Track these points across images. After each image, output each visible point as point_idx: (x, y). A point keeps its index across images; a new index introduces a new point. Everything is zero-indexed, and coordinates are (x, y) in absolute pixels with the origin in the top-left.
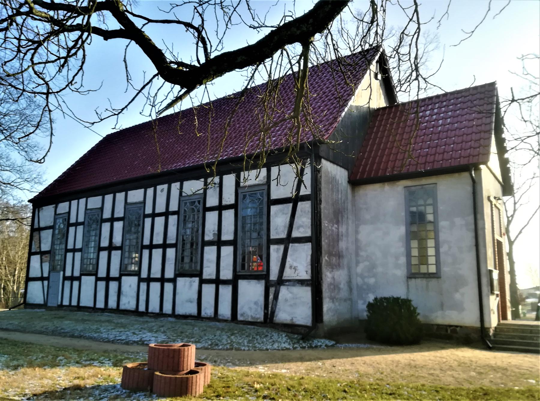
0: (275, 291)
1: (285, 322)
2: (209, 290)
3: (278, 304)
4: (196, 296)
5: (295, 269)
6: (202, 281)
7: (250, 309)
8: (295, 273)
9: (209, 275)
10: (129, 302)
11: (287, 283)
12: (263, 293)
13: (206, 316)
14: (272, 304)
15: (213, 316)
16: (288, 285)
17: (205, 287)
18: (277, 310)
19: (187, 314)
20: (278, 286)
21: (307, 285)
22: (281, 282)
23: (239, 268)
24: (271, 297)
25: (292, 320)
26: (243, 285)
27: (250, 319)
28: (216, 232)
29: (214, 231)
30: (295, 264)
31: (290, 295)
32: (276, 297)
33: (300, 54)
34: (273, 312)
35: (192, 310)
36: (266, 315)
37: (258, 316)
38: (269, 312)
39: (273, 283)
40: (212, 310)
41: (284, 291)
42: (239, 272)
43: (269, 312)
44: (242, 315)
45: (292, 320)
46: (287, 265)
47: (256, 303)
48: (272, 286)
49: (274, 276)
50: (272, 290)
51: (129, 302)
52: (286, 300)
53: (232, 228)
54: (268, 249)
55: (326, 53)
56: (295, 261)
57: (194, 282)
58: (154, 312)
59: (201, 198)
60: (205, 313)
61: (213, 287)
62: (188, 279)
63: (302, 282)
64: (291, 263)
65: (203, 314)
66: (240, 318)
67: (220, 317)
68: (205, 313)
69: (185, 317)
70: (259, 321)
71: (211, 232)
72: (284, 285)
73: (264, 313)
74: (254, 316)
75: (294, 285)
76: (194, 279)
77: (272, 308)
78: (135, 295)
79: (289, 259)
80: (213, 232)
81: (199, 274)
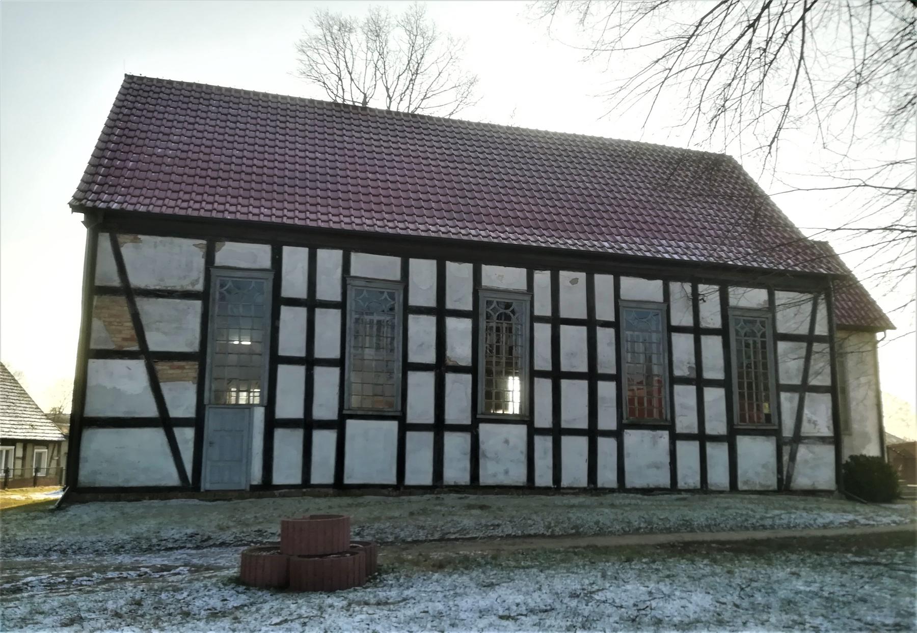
0: (791, 450)
1: (806, 488)
2: (688, 452)
3: (796, 466)
4: (667, 460)
5: (815, 423)
6: (675, 437)
7: (757, 474)
8: (815, 428)
9: (687, 427)
10: (507, 472)
11: (806, 441)
12: (775, 453)
13: (686, 487)
14: (788, 467)
15: (699, 486)
16: (807, 443)
17: (681, 445)
18: (795, 473)
19: (651, 486)
20: (794, 445)
21: (830, 443)
22: (798, 438)
23: (736, 419)
24: (786, 458)
25: (814, 484)
26: (744, 443)
27: (758, 488)
28: (694, 366)
29: (689, 363)
30: (814, 418)
31: (811, 455)
32: (793, 458)
33: (879, 345)
34: (789, 477)
35: (518, 476)
36: (780, 481)
37: (769, 483)
38: (785, 478)
39: (787, 440)
40: (698, 478)
41: (803, 452)
42: (738, 425)
43: (785, 478)
44: (746, 483)
45: (814, 484)
46: (805, 418)
47: (764, 466)
48: (786, 444)
49: (788, 431)
50: (786, 450)
51: (507, 472)
52: (806, 462)
53: (721, 362)
54: (778, 396)
55: (758, 18)
56: (814, 413)
57: (661, 437)
58: (575, 486)
59: (661, 310)
60: (685, 484)
61: (695, 446)
62: (647, 433)
63: (823, 440)
64: (809, 415)
65: (681, 484)
66: (741, 486)
67: (713, 488)
68: (685, 484)
69: (647, 491)
70: (771, 489)
71: (685, 363)
72: (803, 443)
73: (778, 479)
74: (763, 483)
75: (814, 444)
76: (659, 432)
77: (788, 472)
78: (523, 458)
79: (806, 411)
80: (688, 365)
81: (670, 427)
